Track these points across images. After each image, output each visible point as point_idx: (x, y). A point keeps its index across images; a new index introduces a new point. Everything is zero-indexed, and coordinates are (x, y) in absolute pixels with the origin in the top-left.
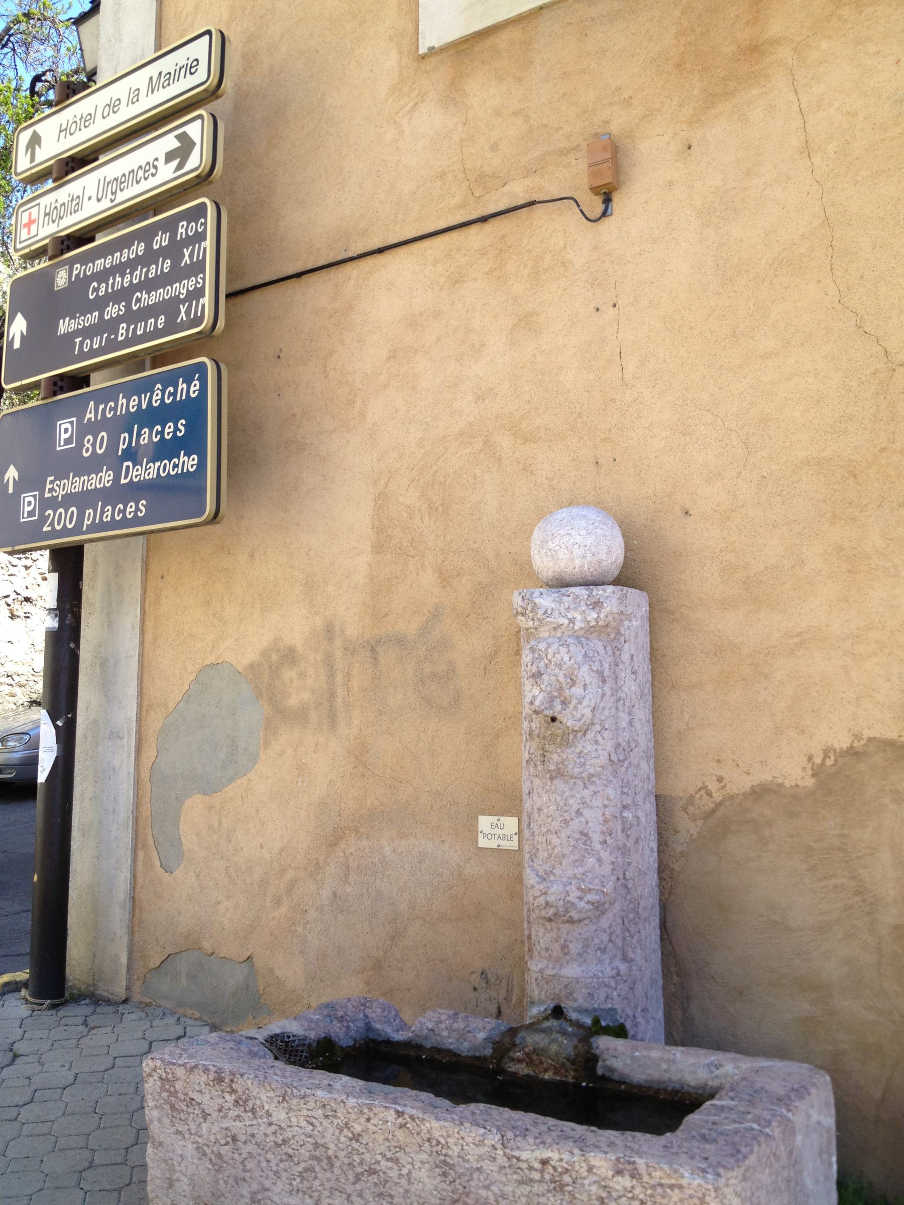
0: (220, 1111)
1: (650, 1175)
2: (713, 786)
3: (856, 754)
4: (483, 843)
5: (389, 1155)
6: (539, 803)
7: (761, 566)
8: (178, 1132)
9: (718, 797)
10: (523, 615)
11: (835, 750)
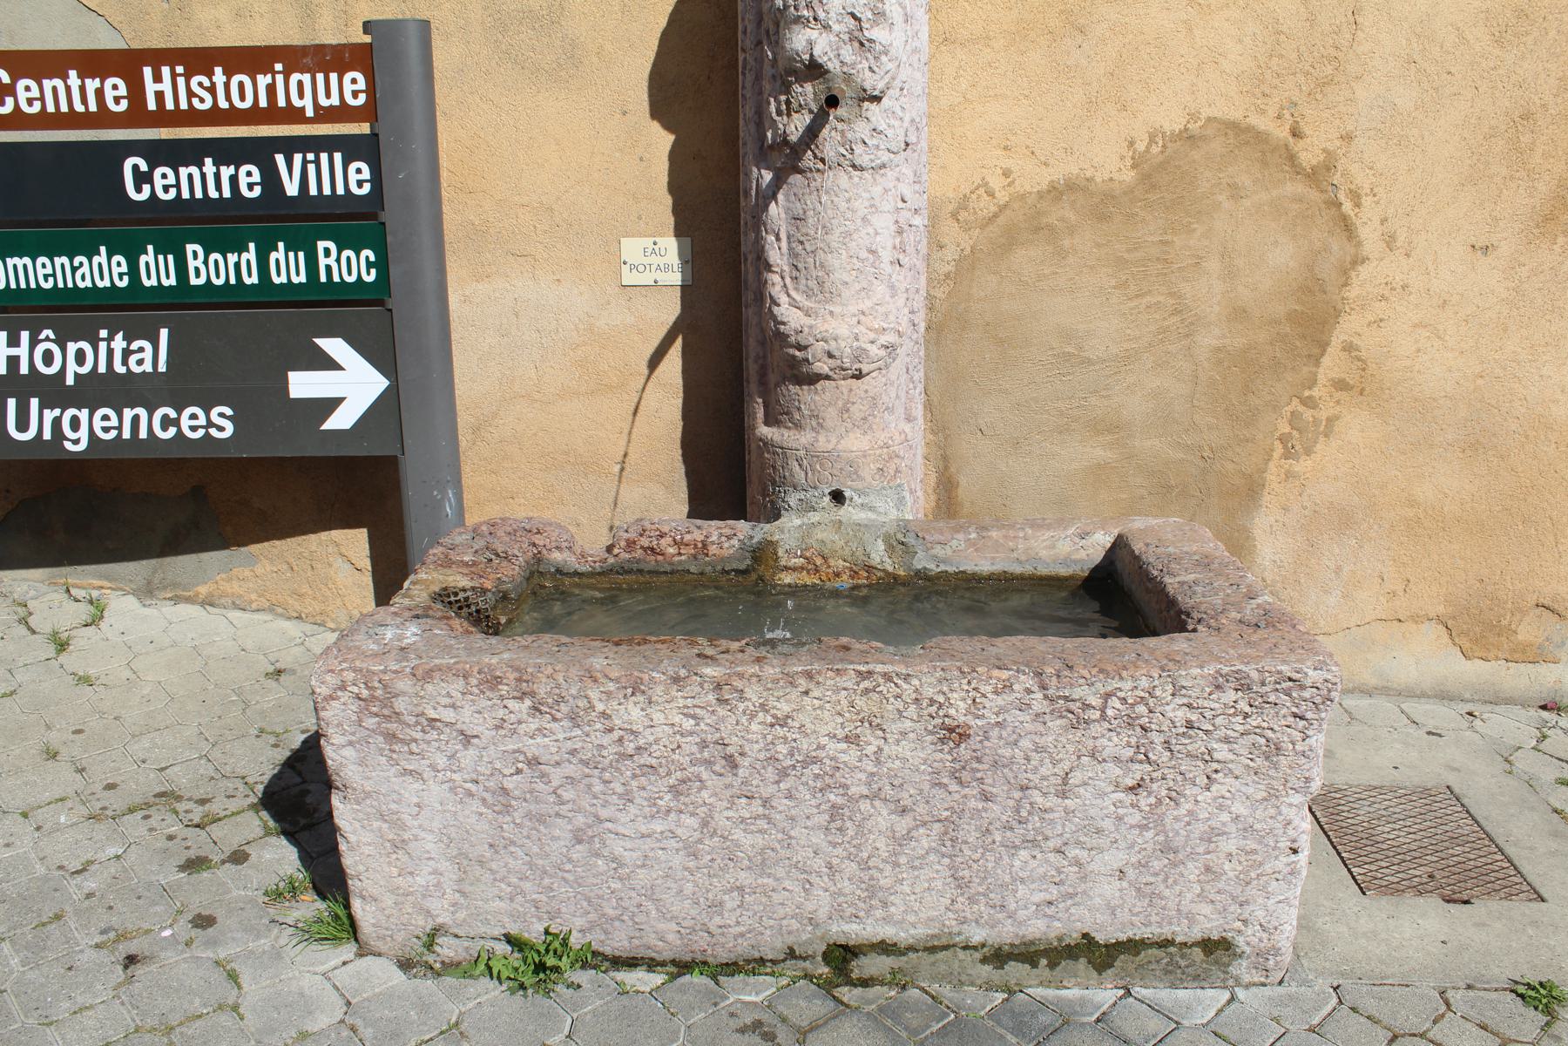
0: (497, 727)
2: (996, 182)
8: (406, 772)
9: (1002, 197)
11: (1164, 134)
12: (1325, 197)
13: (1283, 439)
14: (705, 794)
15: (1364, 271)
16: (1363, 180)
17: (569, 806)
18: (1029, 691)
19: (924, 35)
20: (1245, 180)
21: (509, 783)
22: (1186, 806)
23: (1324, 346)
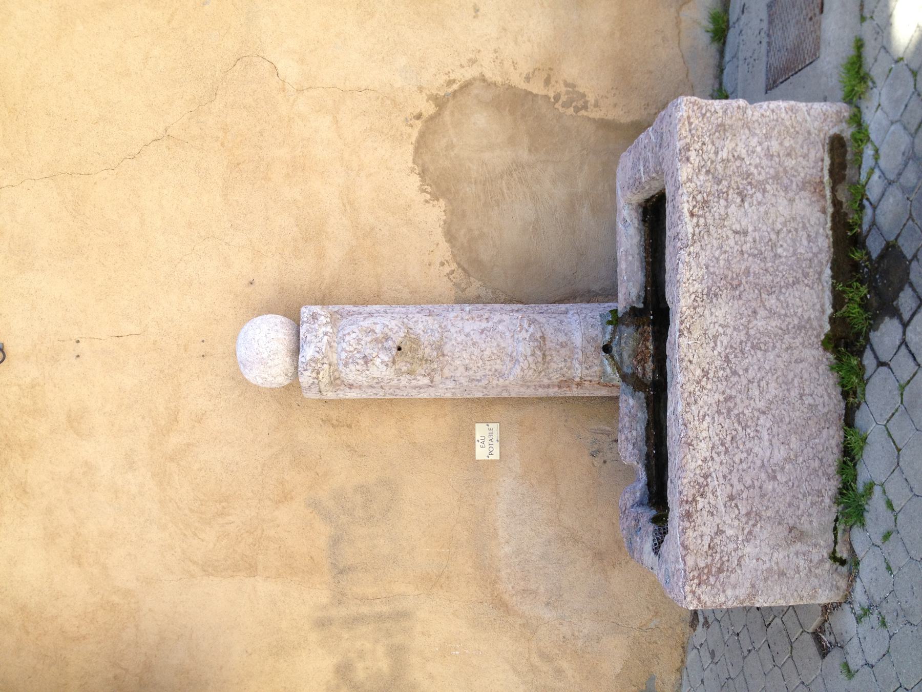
0: (712, 515)
1: (685, 137)
2: (447, 269)
3: (423, 171)
4: (496, 456)
5: (712, 344)
6: (462, 369)
7: (295, 229)
8: (739, 565)
9: (454, 266)
10: (318, 373)
12: (449, 100)
13: (577, 110)
14: (746, 412)
15: (488, 75)
16: (443, 79)
17: (756, 482)
18: (689, 254)
19: (377, 307)
20: (444, 142)
21: (744, 512)
22: (752, 169)
23: (528, 93)
